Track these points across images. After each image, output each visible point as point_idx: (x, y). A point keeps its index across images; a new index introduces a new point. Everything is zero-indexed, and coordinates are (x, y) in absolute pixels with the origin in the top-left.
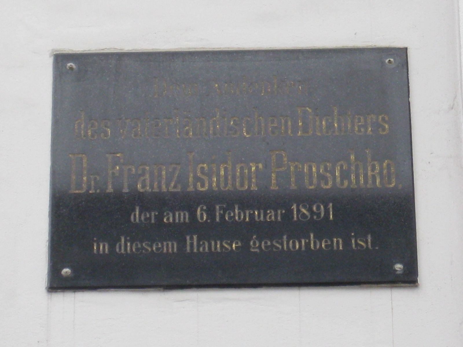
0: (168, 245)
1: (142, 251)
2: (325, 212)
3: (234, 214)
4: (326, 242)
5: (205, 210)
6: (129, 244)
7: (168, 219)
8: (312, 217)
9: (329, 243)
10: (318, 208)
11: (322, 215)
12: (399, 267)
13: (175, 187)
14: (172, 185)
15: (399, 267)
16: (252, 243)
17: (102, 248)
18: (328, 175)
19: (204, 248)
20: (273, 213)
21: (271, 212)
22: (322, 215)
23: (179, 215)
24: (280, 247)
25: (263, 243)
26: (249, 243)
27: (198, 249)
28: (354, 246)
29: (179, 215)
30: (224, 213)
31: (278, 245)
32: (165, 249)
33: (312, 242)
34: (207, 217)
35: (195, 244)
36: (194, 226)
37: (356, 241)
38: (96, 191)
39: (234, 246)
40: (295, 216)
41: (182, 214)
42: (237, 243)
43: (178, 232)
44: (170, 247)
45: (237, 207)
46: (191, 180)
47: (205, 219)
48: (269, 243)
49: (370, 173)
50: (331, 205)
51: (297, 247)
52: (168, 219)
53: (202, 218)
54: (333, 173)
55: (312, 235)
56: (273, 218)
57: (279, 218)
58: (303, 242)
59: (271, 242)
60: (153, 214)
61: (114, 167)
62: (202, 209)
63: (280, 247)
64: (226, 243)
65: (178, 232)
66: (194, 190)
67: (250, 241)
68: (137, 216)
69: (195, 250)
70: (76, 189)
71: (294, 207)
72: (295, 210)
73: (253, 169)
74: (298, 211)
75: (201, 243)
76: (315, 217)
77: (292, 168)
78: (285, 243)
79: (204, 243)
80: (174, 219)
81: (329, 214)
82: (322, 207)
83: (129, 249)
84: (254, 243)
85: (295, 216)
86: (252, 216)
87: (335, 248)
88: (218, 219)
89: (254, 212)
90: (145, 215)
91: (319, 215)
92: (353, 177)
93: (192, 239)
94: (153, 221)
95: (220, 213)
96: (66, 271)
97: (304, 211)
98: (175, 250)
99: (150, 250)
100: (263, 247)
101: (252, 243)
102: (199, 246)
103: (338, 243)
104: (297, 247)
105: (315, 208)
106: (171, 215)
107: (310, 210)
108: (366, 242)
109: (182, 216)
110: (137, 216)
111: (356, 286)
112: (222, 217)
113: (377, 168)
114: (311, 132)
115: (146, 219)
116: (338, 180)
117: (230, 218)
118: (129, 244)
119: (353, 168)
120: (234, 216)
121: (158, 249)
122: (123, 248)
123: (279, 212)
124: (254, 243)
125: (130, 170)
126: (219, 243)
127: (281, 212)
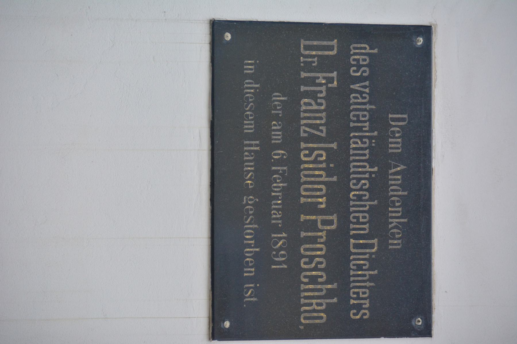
0: (251, 124)
1: (246, 102)
2: (279, 261)
3: (278, 183)
4: (251, 262)
5: (282, 158)
6: (252, 91)
7: (275, 125)
8: (274, 250)
9: (250, 264)
10: (283, 256)
11: (276, 259)
12: (227, 324)
13: (305, 132)
14: (307, 129)
15: (227, 324)
16: (251, 197)
17: (249, 67)
18: (313, 265)
19: (247, 156)
20: (278, 216)
21: (280, 214)
22: (276, 259)
23: (279, 135)
24: (247, 222)
25: (252, 207)
26: (251, 195)
27: (246, 151)
28: (247, 286)
29: (279, 135)
30: (280, 174)
31: (249, 220)
32: (247, 122)
33: (251, 250)
34: (276, 159)
35: (252, 148)
36: (268, 147)
37: (251, 288)
38: (302, 63)
39: (249, 182)
40: (275, 236)
41: (279, 137)
42: (251, 184)
43: (262, 133)
44: (249, 127)
45: (285, 185)
46: (311, 145)
47: (274, 157)
48: (251, 212)
49: (314, 301)
50: (286, 267)
51: (247, 237)
52: (275, 125)
53: (275, 155)
54: (315, 269)
55: (257, 250)
56: (274, 216)
57: (274, 222)
58: (253, 242)
59: (252, 214)
60: (280, 112)
61: (324, 78)
62: (283, 155)
63: (247, 222)
64: (252, 175)
65: (262, 133)
66: (302, 147)
67: (253, 196)
68: (278, 98)
69: (245, 148)
70: (304, 45)
71: (284, 235)
72: (281, 236)
73: (320, 200)
74: (280, 239)
75: (252, 154)
76: (274, 253)
77: (320, 234)
78: (251, 226)
79: (252, 156)
80: (274, 130)
81: (276, 265)
82: (284, 259)
83: (248, 91)
84: (250, 200)
85: (275, 236)
86: (276, 198)
87: (245, 269)
88: (273, 168)
89: (279, 200)
90: (279, 105)
91: (277, 256)
92: (311, 287)
93: (257, 145)
94: (273, 112)
95: (279, 170)
96: (228, 36)
97: (280, 243)
98: (246, 131)
99: (247, 109)
100: (247, 207)
101: (251, 197)
102: (250, 151)
103: (249, 272)
104: (247, 237)
105: (282, 252)
106: (278, 128)
107: (281, 249)
108: (250, 297)
109: (277, 137)
110: (278, 98)
111: (210, 286)
112: (276, 172)
113: (319, 308)
114: (353, 251)
115: (275, 106)
116: (308, 273)
117: (275, 179)
118: (252, 91)
119: (319, 287)
120: (276, 182)
121: (247, 116)
122: (249, 85)
123: (280, 222)
124: (250, 200)
125: (321, 92)
126: (252, 169)
127: (280, 223)
